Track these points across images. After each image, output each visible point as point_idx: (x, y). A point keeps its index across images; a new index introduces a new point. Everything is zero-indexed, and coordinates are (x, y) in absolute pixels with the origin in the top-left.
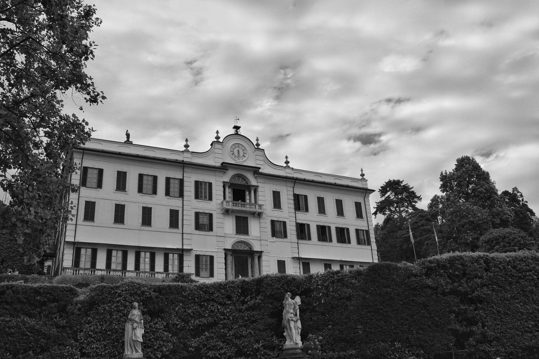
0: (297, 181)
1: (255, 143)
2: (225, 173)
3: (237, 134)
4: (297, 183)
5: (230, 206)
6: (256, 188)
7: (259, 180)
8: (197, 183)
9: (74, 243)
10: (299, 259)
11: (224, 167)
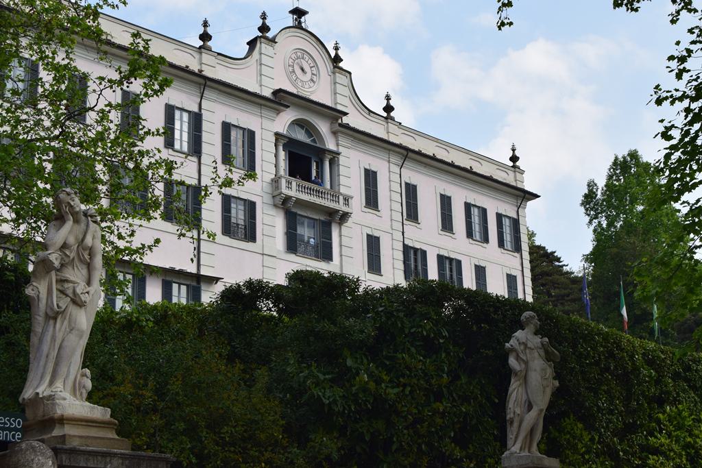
0: (410, 154)
1: (333, 54)
3: (299, 26)
4: (410, 158)
6: (334, 157)
7: (342, 141)
11: (280, 100)
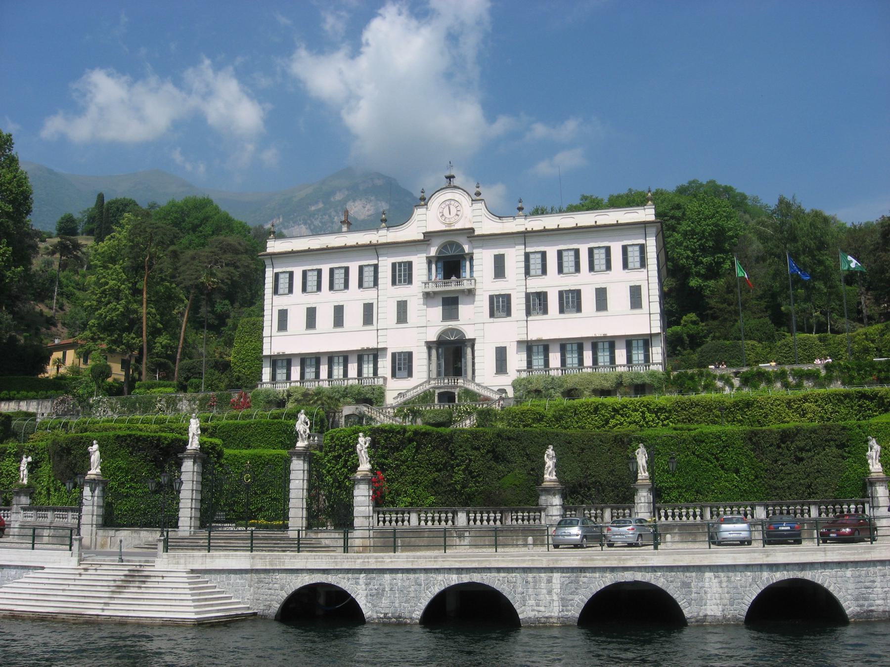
2: (429, 245)
5: (432, 288)
8: (394, 265)
9: (270, 356)
10: (527, 342)
11: (429, 236)
